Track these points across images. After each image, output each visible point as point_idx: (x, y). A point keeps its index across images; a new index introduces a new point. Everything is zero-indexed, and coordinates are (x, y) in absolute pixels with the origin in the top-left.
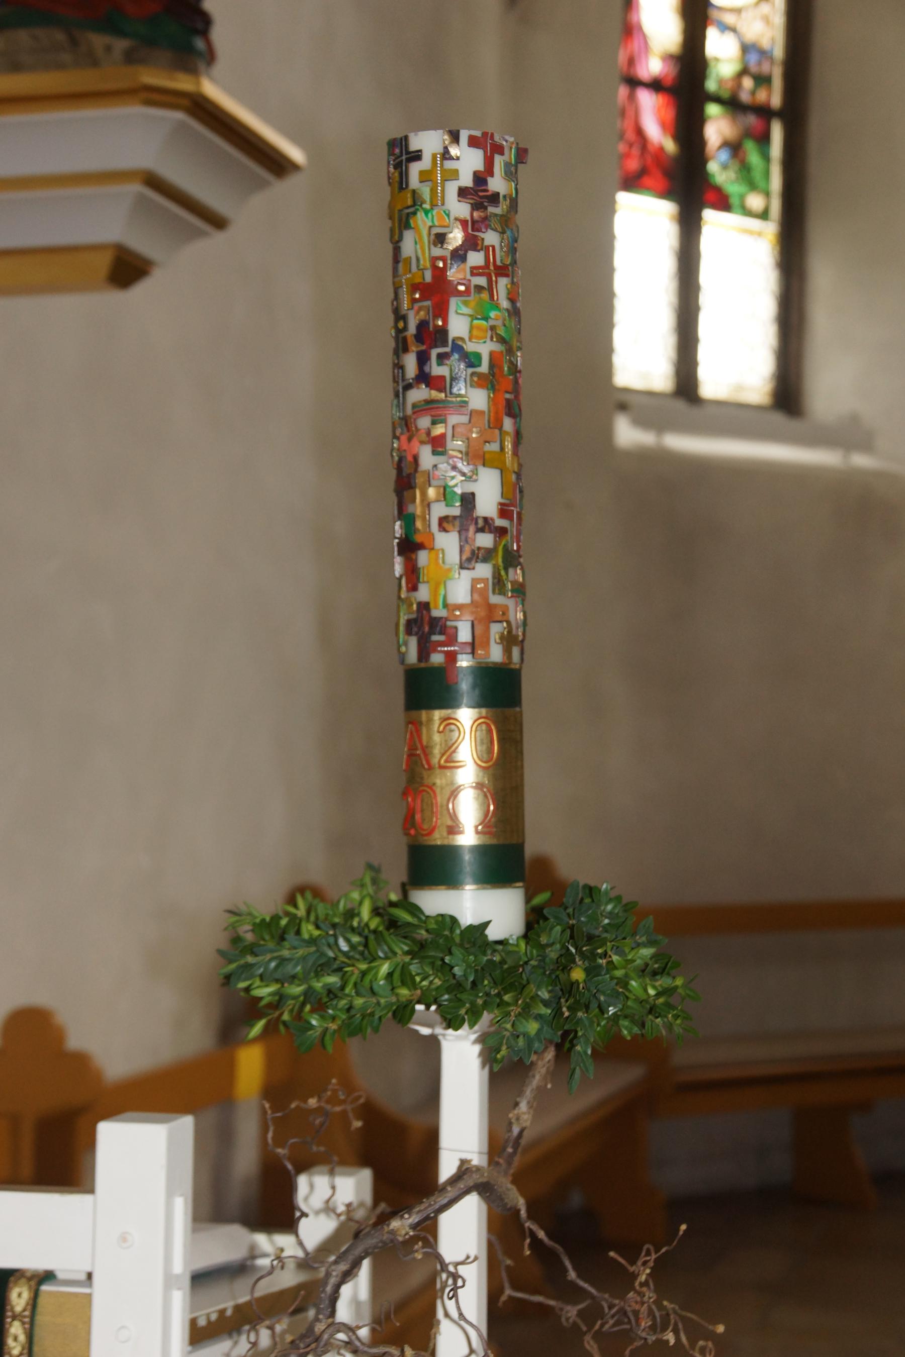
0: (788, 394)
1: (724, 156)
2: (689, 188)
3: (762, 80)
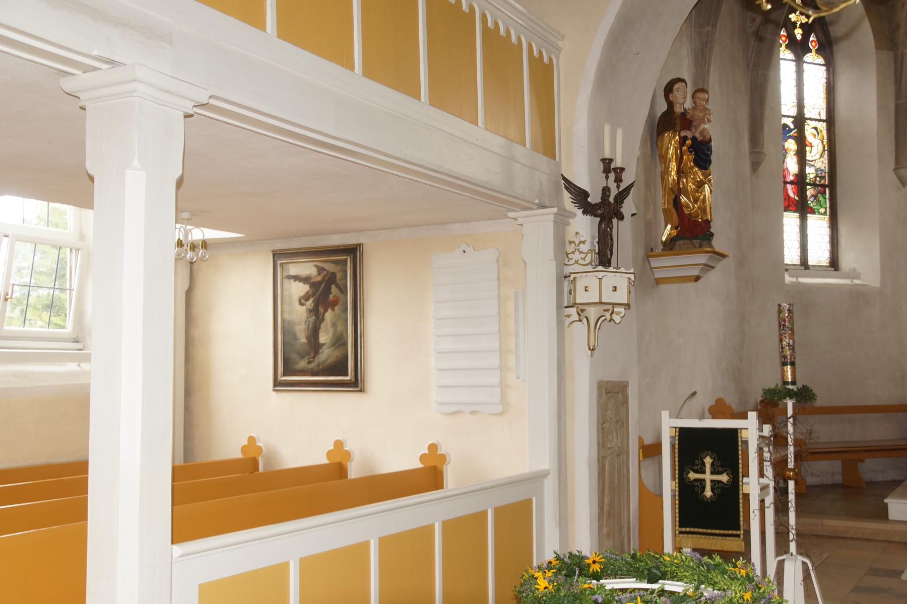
0: (834, 263)
2: (802, 208)
3: (823, 178)
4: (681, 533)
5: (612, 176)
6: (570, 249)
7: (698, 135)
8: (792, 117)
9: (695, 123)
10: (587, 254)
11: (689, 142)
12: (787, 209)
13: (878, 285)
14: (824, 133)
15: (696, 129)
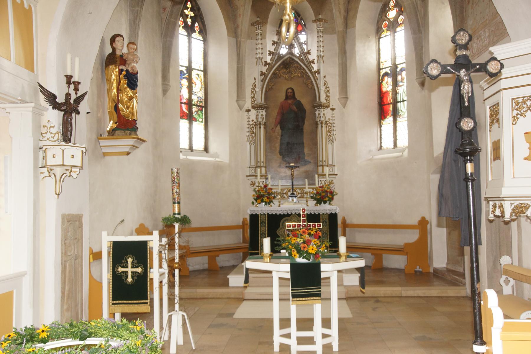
0: (206, 149)
1: (195, 113)
2: (190, 117)
4: (113, 304)
5: (72, 86)
6: (44, 130)
7: (129, 69)
8: (186, 67)
9: (128, 62)
10: (55, 134)
11: (124, 73)
12: (182, 118)
13: (228, 162)
14: (202, 77)
15: (129, 65)
